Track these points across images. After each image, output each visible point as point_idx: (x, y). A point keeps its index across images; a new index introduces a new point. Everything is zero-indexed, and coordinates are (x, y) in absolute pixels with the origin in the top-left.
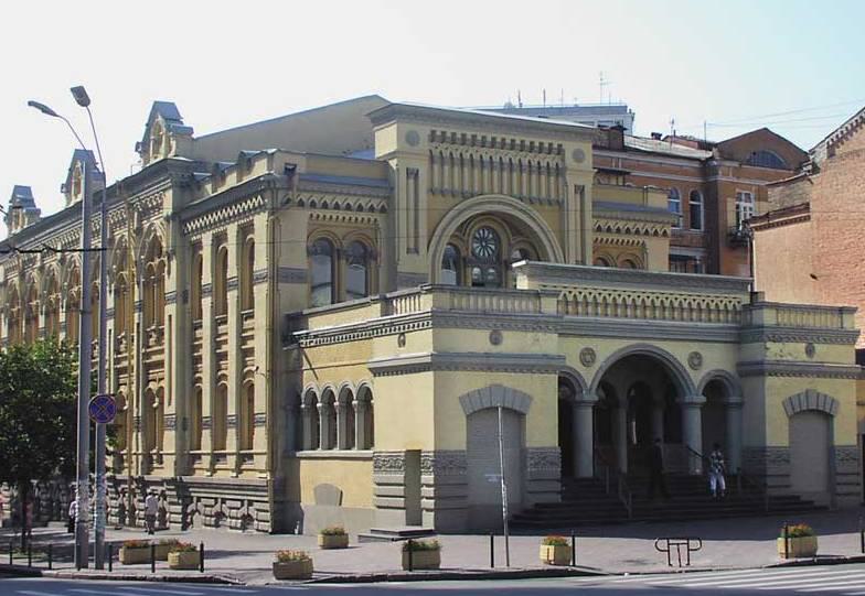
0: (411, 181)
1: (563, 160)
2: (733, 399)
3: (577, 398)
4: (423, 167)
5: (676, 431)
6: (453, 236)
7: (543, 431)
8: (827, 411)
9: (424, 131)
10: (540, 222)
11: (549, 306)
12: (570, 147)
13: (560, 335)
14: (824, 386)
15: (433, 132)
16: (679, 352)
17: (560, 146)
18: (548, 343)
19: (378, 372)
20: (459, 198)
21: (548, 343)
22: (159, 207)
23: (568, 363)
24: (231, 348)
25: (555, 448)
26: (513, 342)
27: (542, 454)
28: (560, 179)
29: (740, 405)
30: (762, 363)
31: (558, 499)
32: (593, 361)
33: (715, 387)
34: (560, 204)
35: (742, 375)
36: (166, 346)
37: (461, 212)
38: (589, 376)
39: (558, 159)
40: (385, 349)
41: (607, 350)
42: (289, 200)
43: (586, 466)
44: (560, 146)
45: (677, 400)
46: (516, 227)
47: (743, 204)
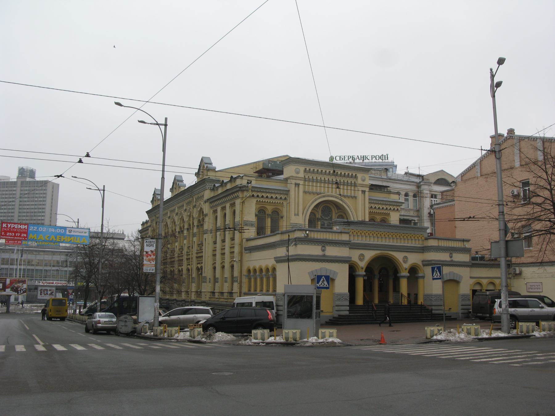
0: (297, 188)
2: (420, 274)
4: (301, 182)
5: (397, 288)
6: (313, 209)
7: (341, 286)
9: (302, 169)
10: (348, 204)
11: (345, 237)
12: (360, 176)
13: (350, 248)
15: (306, 169)
16: (399, 256)
17: (356, 175)
19: (279, 260)
22: (203, 196)
23: (353, 259)
24: (227, 251)
26: (332, 251)
27: (340, 296)
29: (423, 277)
30: (431, 261)
31: (347, 313)
33: (413, 270)
34: (355, 197)
35: (424, 265)
36: (204, 251)
37: (316, 200)
38: (363, 264)
39: (355, 180)
40: (281, 252)
41: (369, 255)
43: (360, 301)
44: (356, 175)
45: (398, 275)
46: (338, 206)
47: (433, 199)
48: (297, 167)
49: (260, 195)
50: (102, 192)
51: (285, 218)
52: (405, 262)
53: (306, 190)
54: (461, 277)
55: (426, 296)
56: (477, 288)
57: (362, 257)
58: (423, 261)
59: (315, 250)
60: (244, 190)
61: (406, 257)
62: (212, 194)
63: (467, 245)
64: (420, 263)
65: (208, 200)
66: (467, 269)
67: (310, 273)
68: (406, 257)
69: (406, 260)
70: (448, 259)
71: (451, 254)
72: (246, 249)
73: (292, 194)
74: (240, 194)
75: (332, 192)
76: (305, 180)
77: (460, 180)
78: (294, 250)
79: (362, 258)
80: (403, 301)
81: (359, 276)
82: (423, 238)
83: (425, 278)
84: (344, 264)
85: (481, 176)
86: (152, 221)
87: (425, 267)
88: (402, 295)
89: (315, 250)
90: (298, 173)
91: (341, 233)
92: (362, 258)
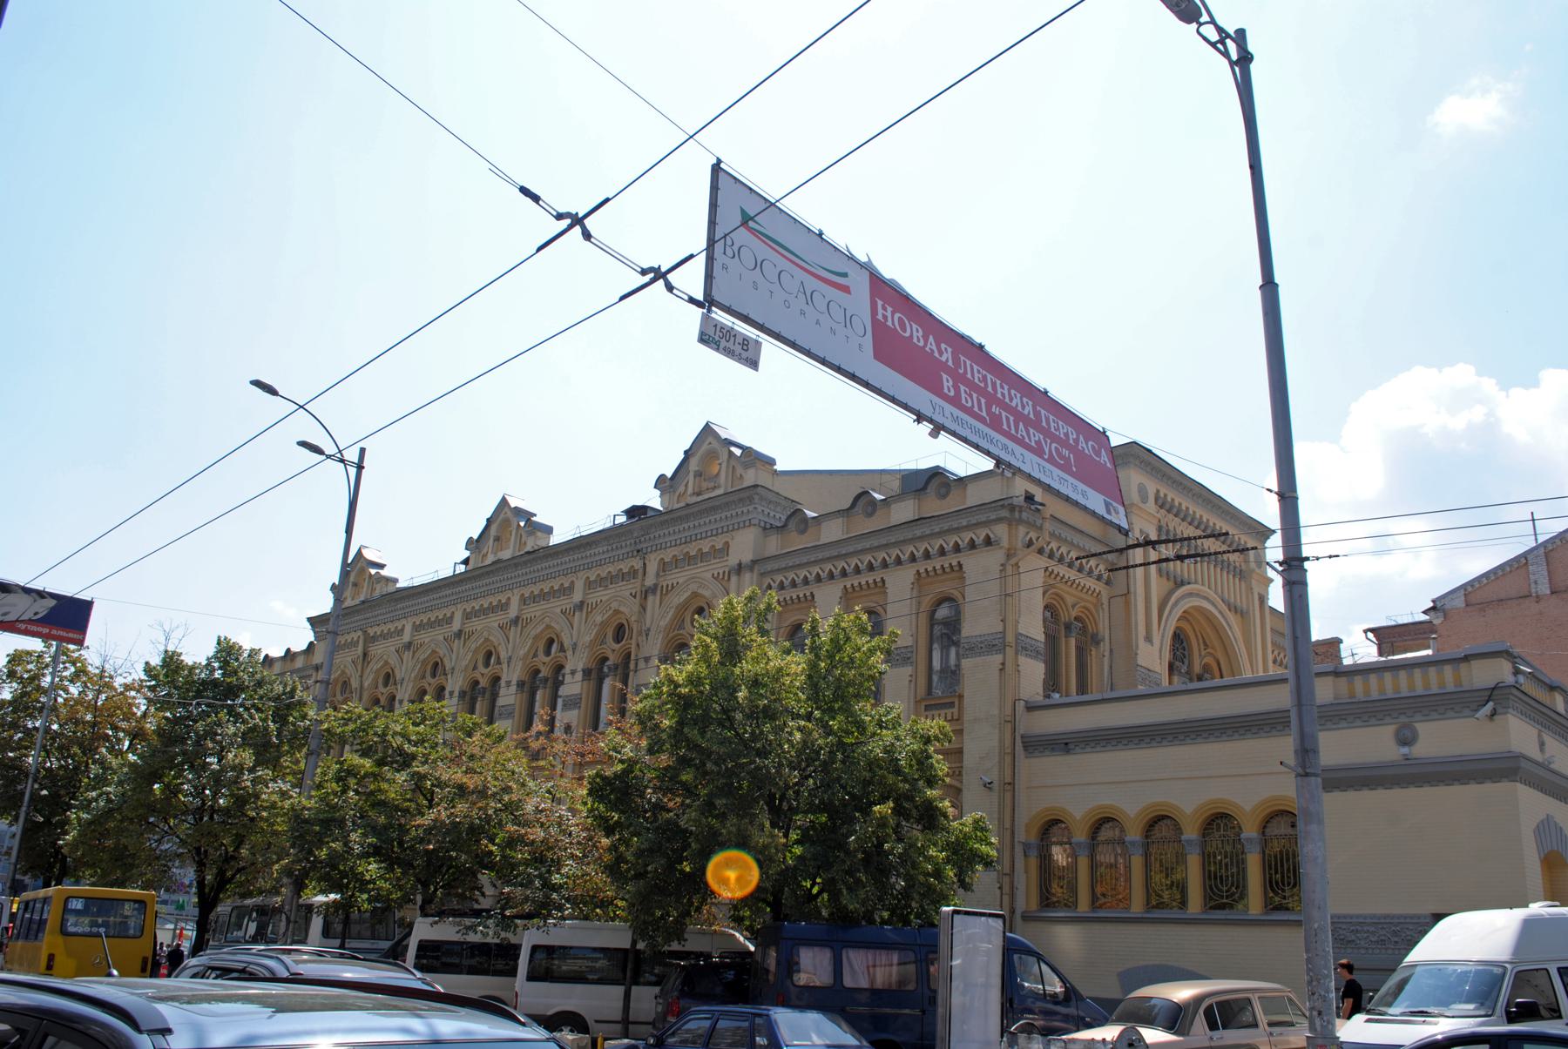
20: (1171, 584)
42: (1030, 544)
50: (353, 471)
51: (1105, 647)
60: (1020, 521)
62: (773, 545)
65: (754, 562)
72: (1037, 745)
74: (1000, 531)
78: (1439, 738)
86: (334, 650)
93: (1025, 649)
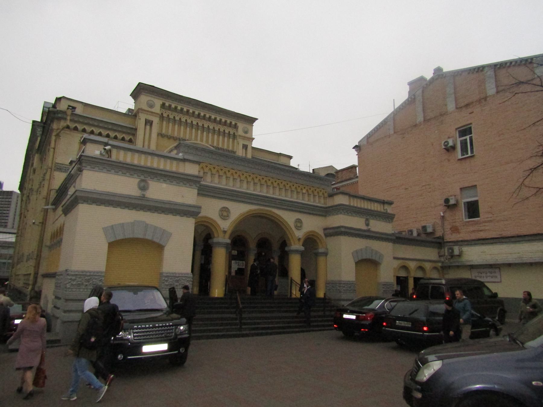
1: (237, 131)
2: (321, 250)
3: (215, 240)
4: (156, 120)
7: (178, 259)
8: (377, 259)
9: (158, 102)
12: (241, 126)
14: (376, 245)
16: (289, 218)
17: (236, 124)
18: (187, 196)
21: (187, 196)
25: (188, 274)
26: (159, 191)
28: (235, 141)
29: (326, 254)
32: (228, 216)
33: (310, 241)
35: (327, 235)
38: (225, 226)
41: (238, 210)
44: (236, 124)
45: (287, 249)
48: (152, 99)
49: (88, 129)
52: (298, 228)
53: (164, 132)
54: (381, 256)
55: (331, 285)
56: (403, 274)
57: (225, 213)
58: (325, 229)
59: (125, 186)
61: (299, 221)
63: (390, 210)
64: (321, 233)
66: (390, 245)
67: (109, 230)
68: (299, 221)
69: (300, 226)
70: (364, 227)
71: (367, 220)
73: (140, 133)
75: (202, 140)
76: (162, 117)
77: (365, 143)
79: (225, 214)
80: (294, 292)
81: (219, 244)
82: (326, 195)
83: (328, 256)
84: (185, 219)
85: (395, 133)
87: (328, 238)
88: (292, 280)
89: (125, 186)
90: (151, 106)
91: (184, 160)
92: (225, 214)
93: (60, 169)
